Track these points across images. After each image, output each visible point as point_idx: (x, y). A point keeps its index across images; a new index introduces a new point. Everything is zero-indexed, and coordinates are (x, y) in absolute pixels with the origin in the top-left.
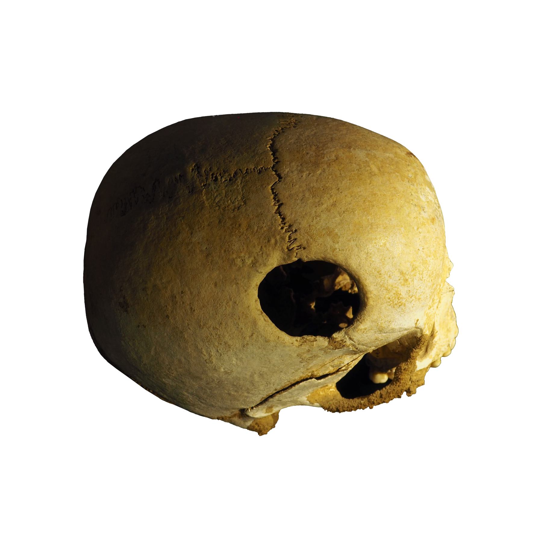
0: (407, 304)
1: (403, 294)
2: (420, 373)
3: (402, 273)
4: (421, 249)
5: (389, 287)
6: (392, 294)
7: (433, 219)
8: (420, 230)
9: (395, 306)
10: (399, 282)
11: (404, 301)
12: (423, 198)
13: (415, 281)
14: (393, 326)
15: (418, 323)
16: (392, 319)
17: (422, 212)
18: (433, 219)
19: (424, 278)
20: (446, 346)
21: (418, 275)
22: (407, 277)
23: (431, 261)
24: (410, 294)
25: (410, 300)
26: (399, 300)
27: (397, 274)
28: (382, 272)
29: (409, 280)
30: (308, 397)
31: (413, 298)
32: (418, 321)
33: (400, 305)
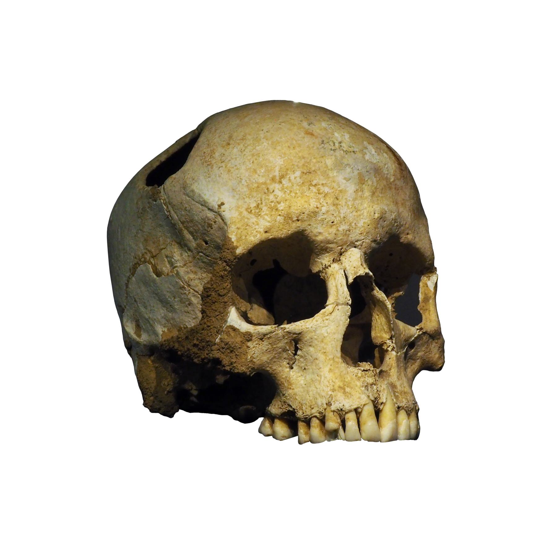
0: (214, 167)
1: (217, 155)
2: (233, 334)
3: (230, 137)
4: (265, 131)
5: (212, 144)
6: (209, 150)
7: (312, 134)
8: (283, 124)
9: (205, 164)
10: (222, 142)
11: (213, 162)
12: (324, 124)
13: (235, 150)
14: (195, 187)
15: (223, 207)
16: (196, 178)
17: (305, 124)
18: (312, 134)
19: (245, 153)
20: (325, 402)
21: (242, 146)
22: (231, 142)
23: (265, 144)
24: (223, 158)
25: (220, 165)
26: (210, 158)
27: (226, 137)
28: (218, 131)
29: (231, 146)
30: (163, 332)
31: (223, 164)
32: (223, 204)
33: (210, 165)
